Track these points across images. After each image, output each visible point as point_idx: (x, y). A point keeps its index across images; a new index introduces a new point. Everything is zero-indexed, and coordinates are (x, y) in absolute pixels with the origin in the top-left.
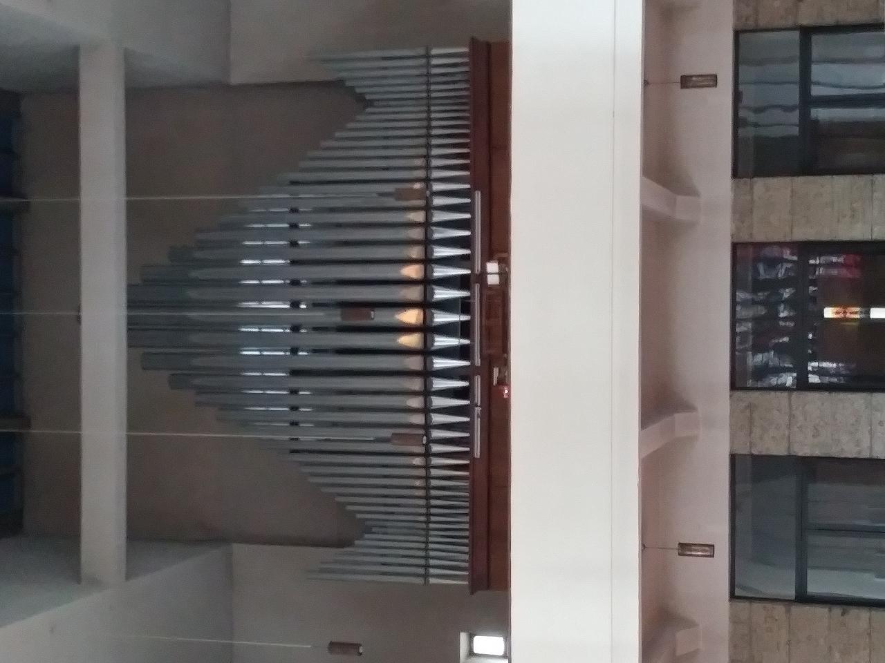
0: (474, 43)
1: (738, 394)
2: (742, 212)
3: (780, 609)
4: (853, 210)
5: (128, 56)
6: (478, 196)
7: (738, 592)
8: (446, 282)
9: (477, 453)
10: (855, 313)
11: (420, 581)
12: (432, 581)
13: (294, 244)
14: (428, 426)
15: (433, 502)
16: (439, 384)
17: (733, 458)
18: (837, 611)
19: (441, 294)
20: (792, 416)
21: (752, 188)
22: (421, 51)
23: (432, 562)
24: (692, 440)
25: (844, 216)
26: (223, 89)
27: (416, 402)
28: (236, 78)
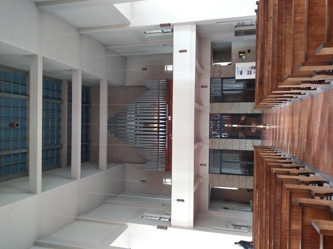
0: (167, 80)
1: (210, 139)
2: (211, 108)
3: (217, 175)
4: (230, 108)
5: (108, 81)
6: (167, 105)
7: (210, 172)
8: (162, 120)
9: (167, 148)
10: (230, 126)
11: (157, 170)
12: (159, 170)
13: (136, 113)
14: (158, 144)
15: (159, 157)
16: (160, 137)
17: (209, 149)
18: (227, 175)
19: (161, 121)
20: (219, 143)
21: (213, 105)
22: (158, 81)
23: (159, 167)
24: (203, 146)
25: (228, 109)
26: (124, 87)
27: (156, 140)
28: (126, 85)
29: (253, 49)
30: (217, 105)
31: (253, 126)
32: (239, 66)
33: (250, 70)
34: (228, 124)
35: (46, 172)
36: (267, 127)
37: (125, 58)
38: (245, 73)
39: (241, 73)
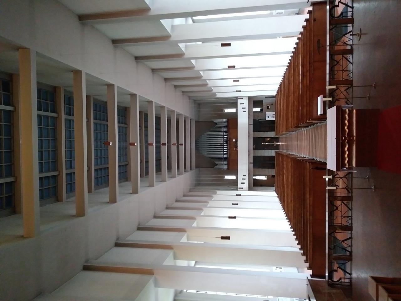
8: (225, 141)
10: (264, 143)
14: (223, 155)
27: (222, 152)
29: (274, 104)
30: (257, 133)
31: (275, 143)
32: (268, 114)
33: (273, 115)
34: (264, 142)
35: (158, 173)
36: (281, 144)
37: (199, 104)
38: (270, 117)
39: (269, 117)
